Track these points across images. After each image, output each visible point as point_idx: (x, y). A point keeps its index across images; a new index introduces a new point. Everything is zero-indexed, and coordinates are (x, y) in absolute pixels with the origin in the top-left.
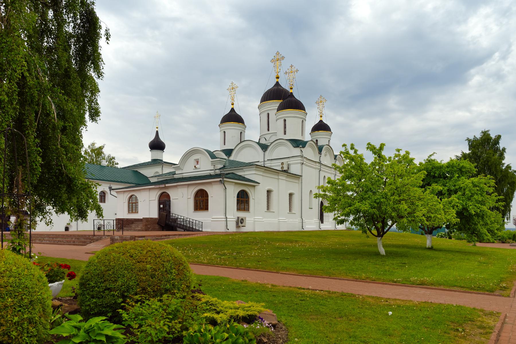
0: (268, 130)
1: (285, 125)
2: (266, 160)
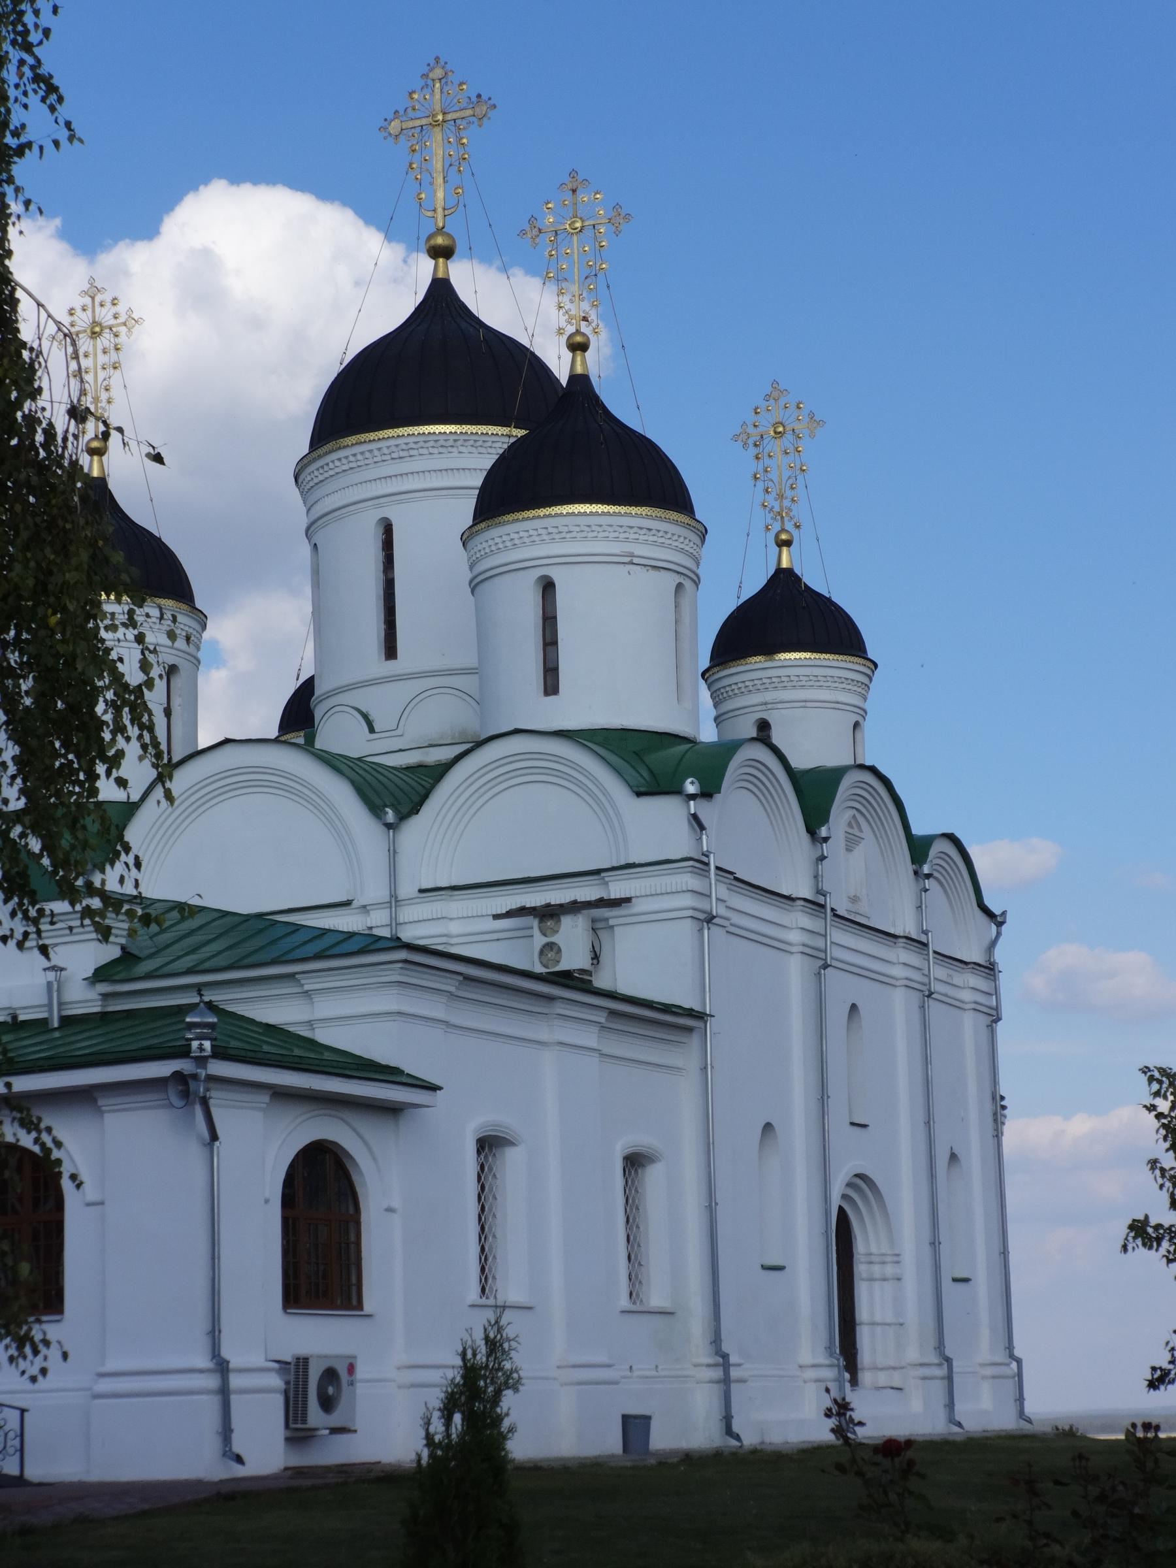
0: (390, 650)
1: (549, 620)
2: (407, 889)
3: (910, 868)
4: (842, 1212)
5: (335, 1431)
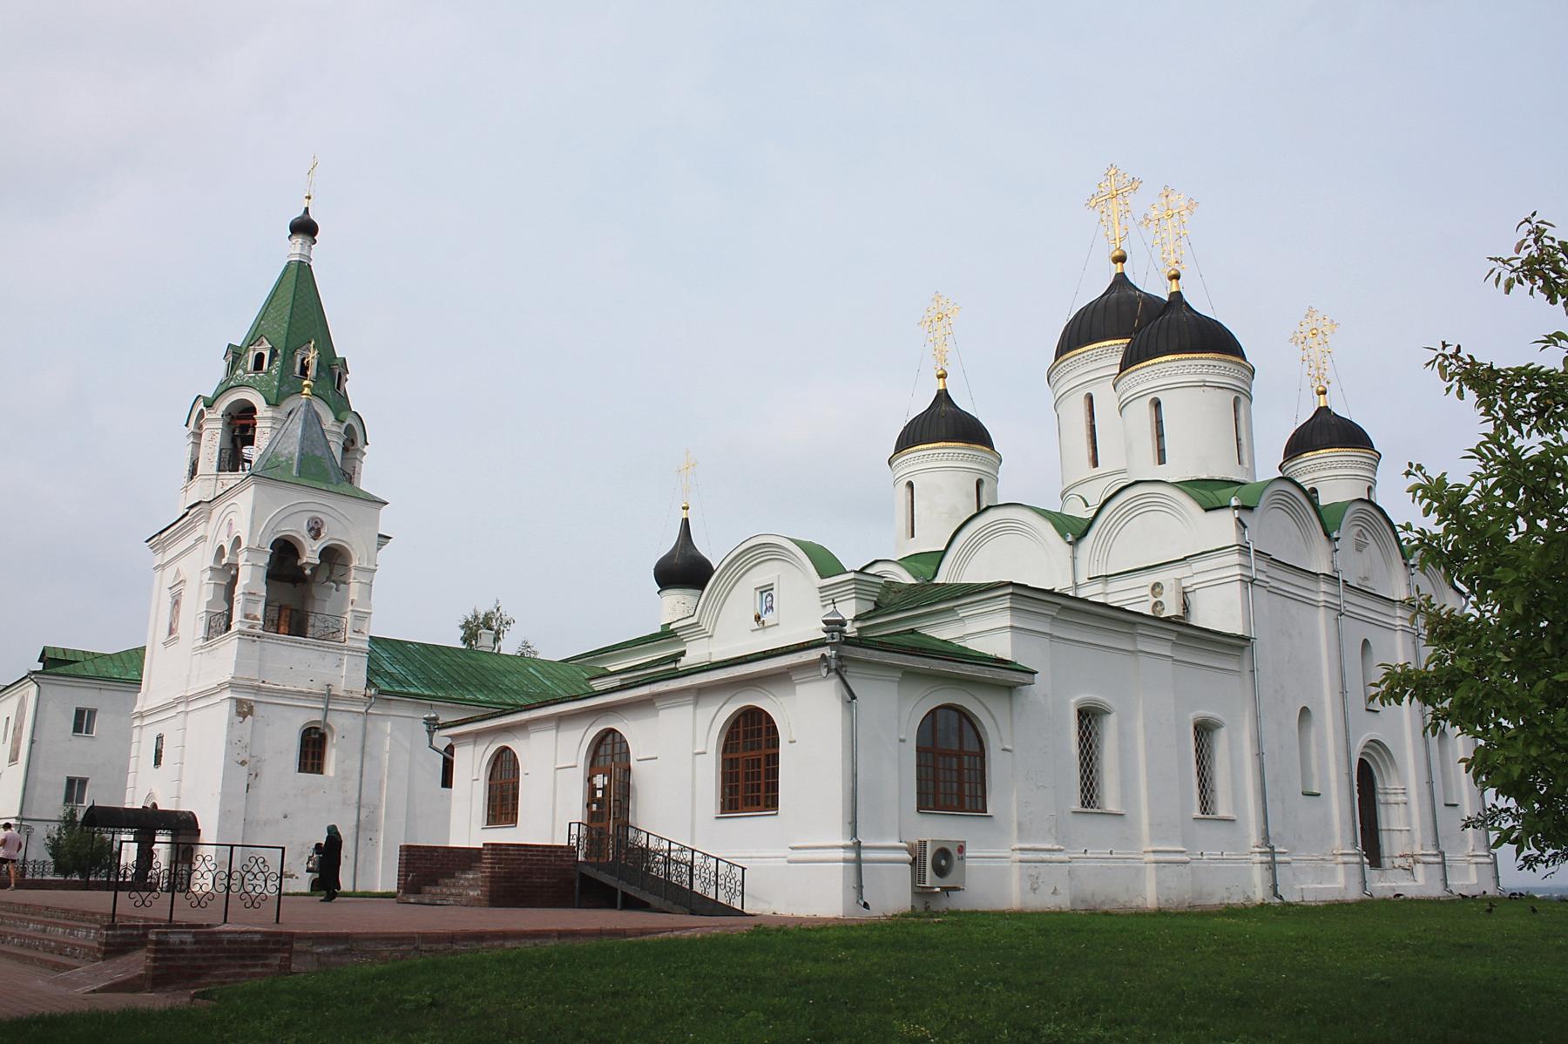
2: (1082, 579)
3: (1401, 562)
4: (1363, 764)
5: (946, 890)
